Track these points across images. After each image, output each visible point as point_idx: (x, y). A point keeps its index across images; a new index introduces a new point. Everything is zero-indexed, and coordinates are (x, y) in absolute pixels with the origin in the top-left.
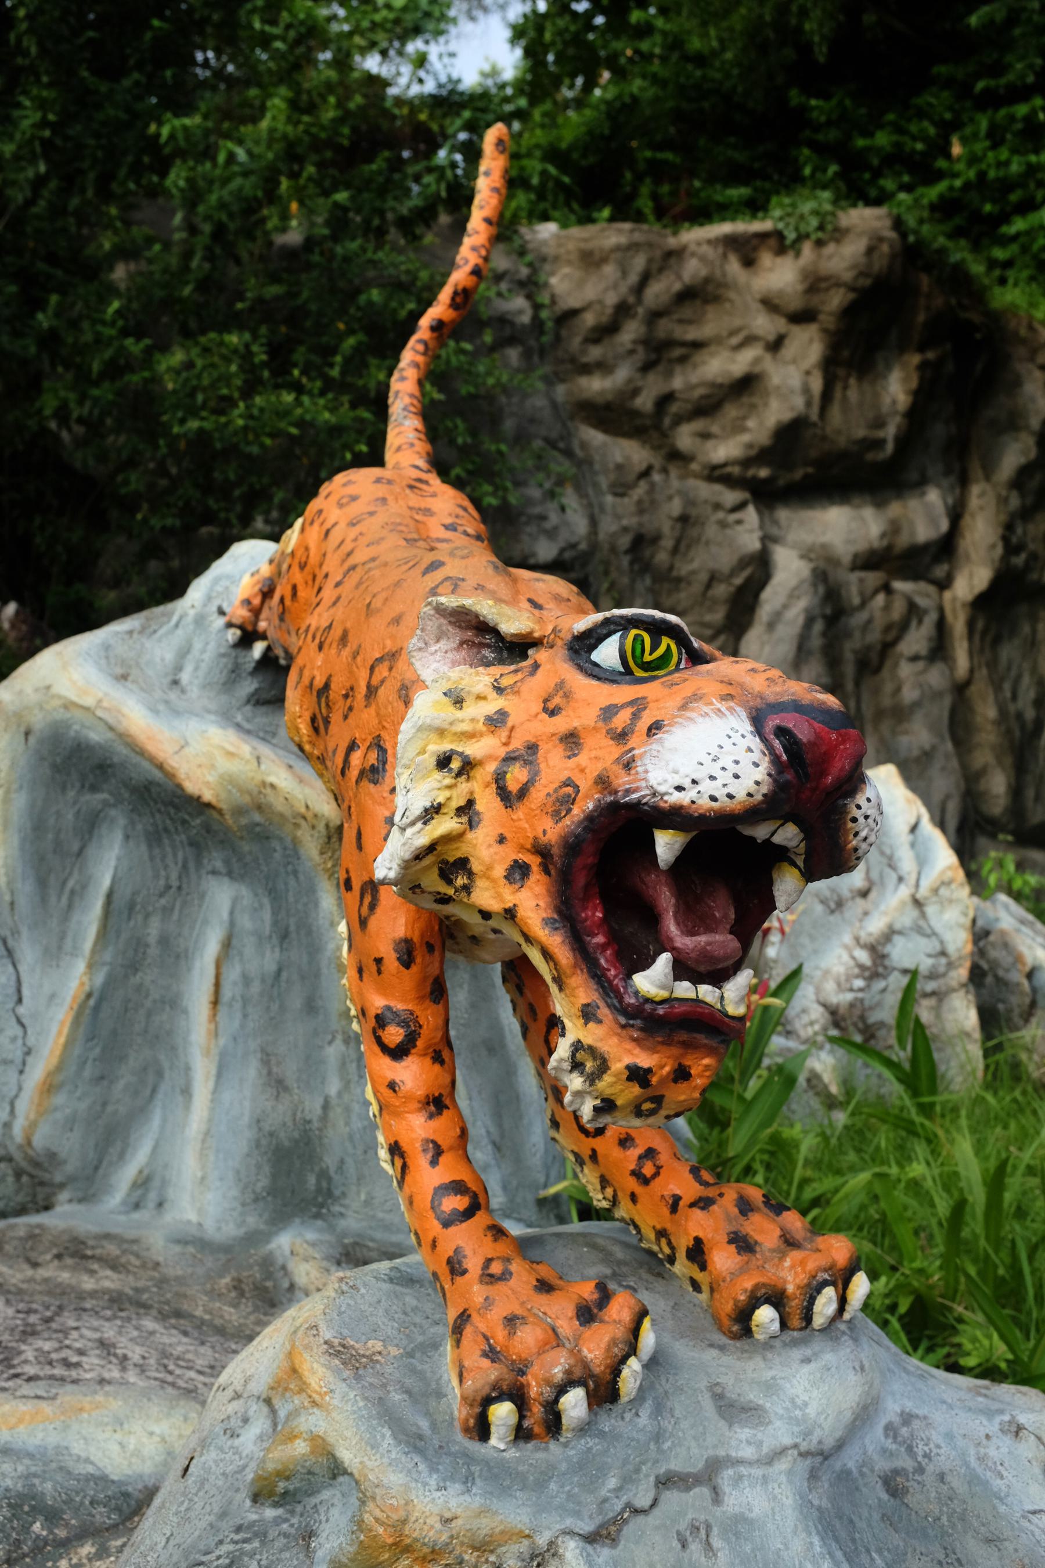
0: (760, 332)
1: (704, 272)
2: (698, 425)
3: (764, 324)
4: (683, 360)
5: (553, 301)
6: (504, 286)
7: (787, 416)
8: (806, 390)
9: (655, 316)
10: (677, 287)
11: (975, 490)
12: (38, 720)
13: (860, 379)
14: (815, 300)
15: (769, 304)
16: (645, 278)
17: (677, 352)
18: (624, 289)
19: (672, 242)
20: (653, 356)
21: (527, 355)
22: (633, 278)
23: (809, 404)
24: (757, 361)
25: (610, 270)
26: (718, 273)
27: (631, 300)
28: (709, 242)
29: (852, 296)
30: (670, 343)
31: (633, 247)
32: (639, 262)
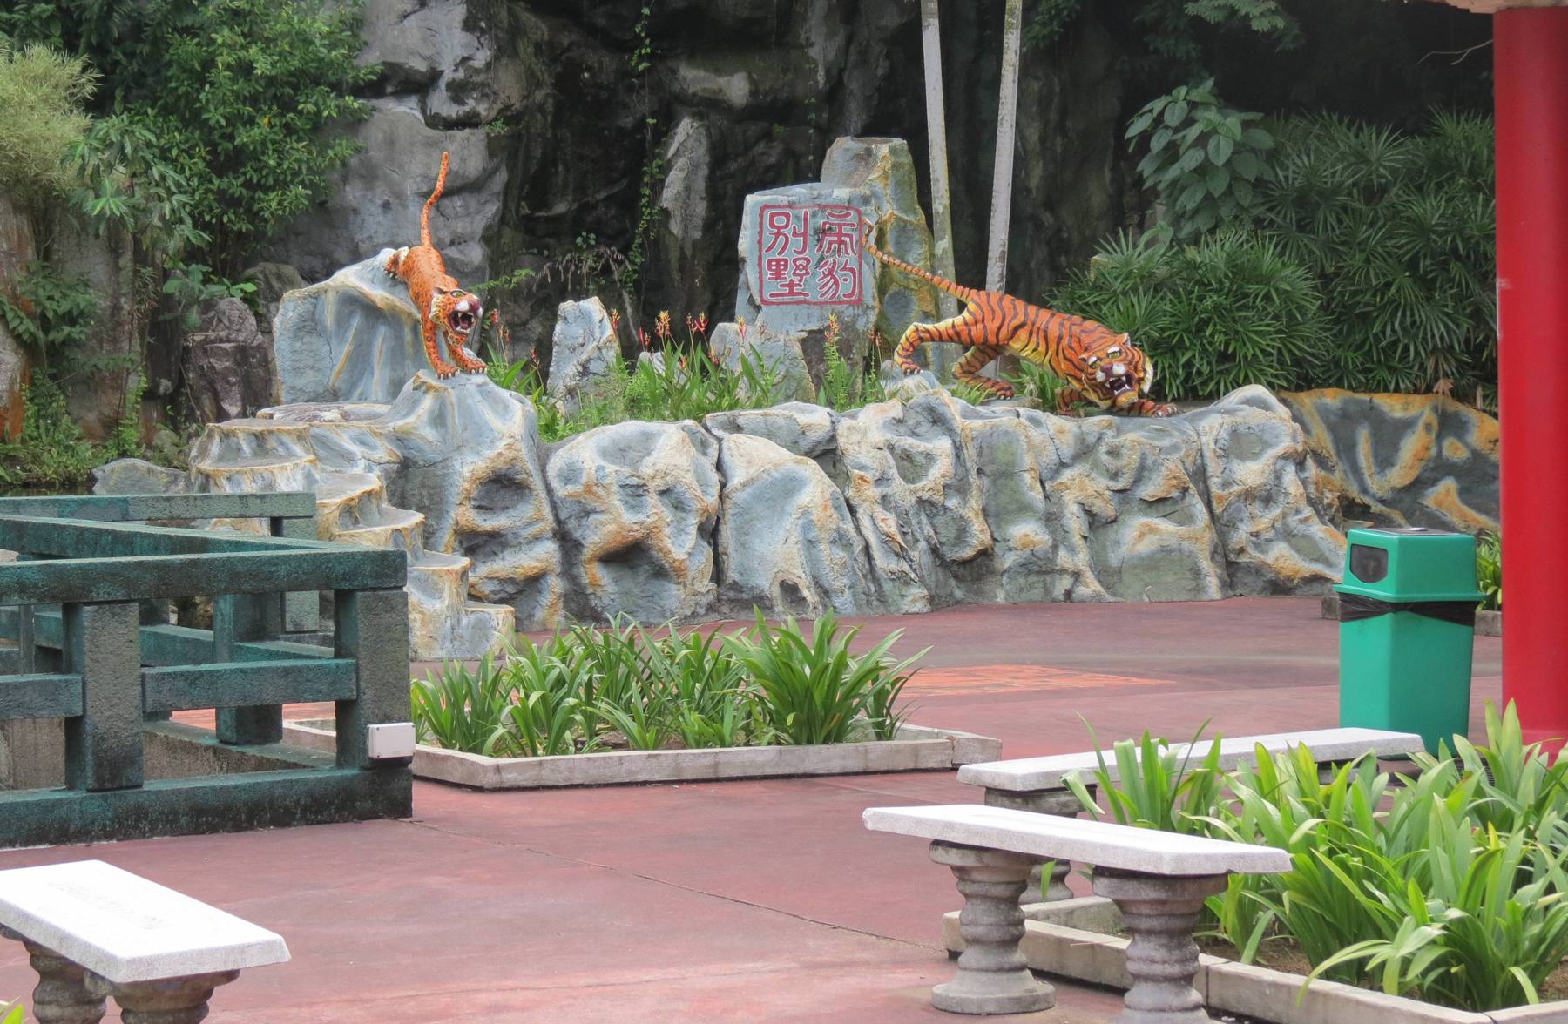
12: (341, 290)
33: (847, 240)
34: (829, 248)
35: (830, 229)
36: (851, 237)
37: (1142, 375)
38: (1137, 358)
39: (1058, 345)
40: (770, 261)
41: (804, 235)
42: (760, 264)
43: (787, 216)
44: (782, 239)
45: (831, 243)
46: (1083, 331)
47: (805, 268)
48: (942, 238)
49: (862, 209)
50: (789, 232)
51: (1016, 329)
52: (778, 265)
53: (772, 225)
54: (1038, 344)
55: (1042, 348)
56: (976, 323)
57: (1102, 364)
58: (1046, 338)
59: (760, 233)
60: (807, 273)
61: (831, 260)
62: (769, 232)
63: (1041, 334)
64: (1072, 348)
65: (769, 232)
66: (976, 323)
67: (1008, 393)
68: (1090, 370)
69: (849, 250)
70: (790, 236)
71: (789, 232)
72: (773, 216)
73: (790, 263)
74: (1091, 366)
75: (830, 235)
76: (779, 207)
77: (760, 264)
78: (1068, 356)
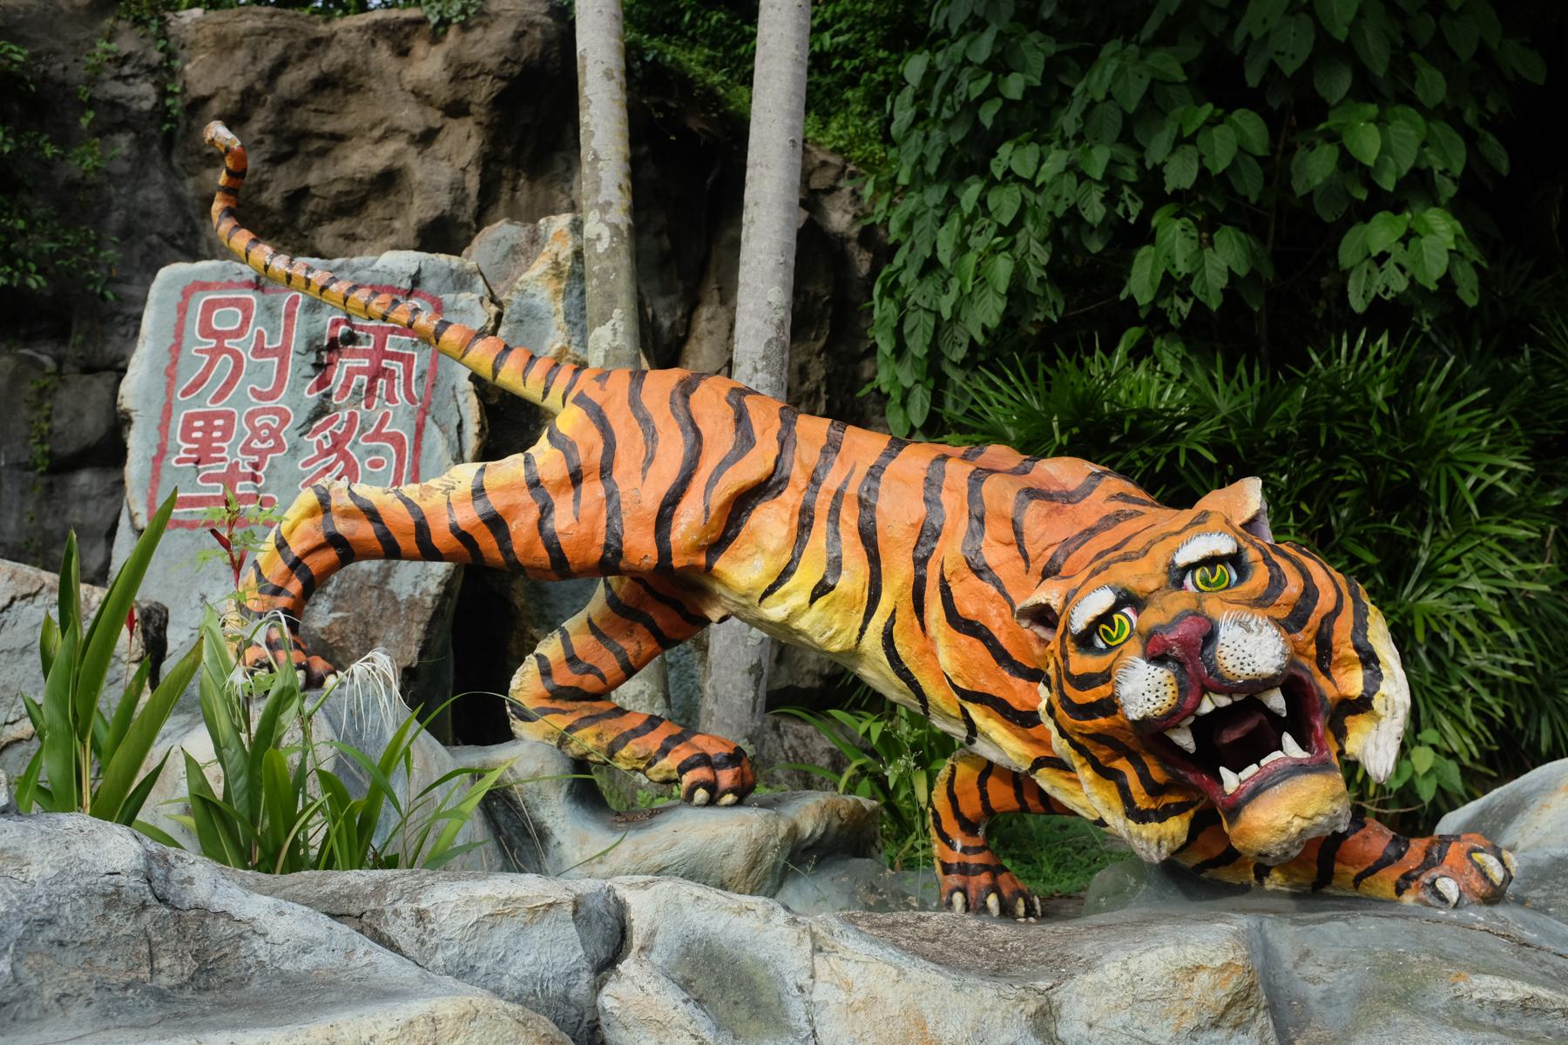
0: (404, 124)
1: (343, 60)
2: (341, 225)
3: (411, 116)
4: (322, 153)
5: (184, 90)
6: (127, 70)
7: (430, 214)
8: (457, 188)
9: (289, 105)
10: (314, 73)
11: (704, 312)
13: (532, 179)
14: (463, 90)
15: (420, 95)
16: (281, 65)
17: (316, 145)
18: (251, 76)
19: (323, 29)
20: (286, 148)
21: (142, 143)
22: (265, 64)
23: (459, 202)
24: (398, 154)
25: (241, 55)
26: (359, 59)
27: (259, 86)
28: (359, 29)
29: (501, 84)
30: (305, 135)
31: (270, 32)
32: (276, 48)
33: (398, 367)
34: (346, 387)
35: (351, 339)
36: (408, 360)
37: (1353, 682)
38: (1326, 601)
39: (921, 563)
40: (189, 419)
41: (282, 353)
42: (164, 428)
43: (246, 306)
44: (225, 363)
45: (350, 374)
46: (1032, 493)
47: (275, 434)
48: (604, 318)
49: (448, 298)
50: (244, 346)
51: (744, 502)
52: (208, 429)
53: (207, 331)
54: (836, 565)
55: (853, 580)
56: (576, 478)
57: (1152, 617)
58: (868, 537)
59: (176, 348)
60: (279, 446)
61: (344, 415)
62: (196, 345)
63: (850, 518)
64: (980, 571)
65: (196, 345)
66: (576, 478)
67: (726, 777)
68: (1082, 663)
69: (400, 393)
70: (247, 356)
71: (244, 346)
72: (210, 306)
73: (240, 423)
74: (1085, 641)
75: (353, 354)
76: (230, 285)
77: (164, 428)
78: (968, 608)
